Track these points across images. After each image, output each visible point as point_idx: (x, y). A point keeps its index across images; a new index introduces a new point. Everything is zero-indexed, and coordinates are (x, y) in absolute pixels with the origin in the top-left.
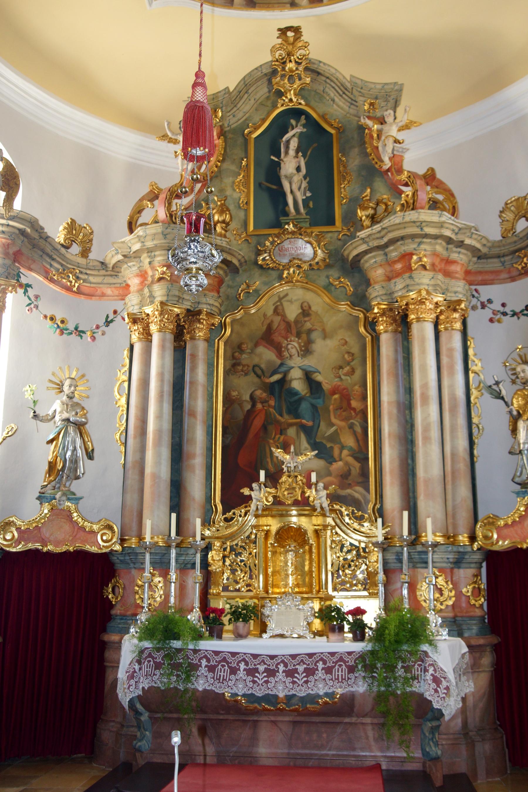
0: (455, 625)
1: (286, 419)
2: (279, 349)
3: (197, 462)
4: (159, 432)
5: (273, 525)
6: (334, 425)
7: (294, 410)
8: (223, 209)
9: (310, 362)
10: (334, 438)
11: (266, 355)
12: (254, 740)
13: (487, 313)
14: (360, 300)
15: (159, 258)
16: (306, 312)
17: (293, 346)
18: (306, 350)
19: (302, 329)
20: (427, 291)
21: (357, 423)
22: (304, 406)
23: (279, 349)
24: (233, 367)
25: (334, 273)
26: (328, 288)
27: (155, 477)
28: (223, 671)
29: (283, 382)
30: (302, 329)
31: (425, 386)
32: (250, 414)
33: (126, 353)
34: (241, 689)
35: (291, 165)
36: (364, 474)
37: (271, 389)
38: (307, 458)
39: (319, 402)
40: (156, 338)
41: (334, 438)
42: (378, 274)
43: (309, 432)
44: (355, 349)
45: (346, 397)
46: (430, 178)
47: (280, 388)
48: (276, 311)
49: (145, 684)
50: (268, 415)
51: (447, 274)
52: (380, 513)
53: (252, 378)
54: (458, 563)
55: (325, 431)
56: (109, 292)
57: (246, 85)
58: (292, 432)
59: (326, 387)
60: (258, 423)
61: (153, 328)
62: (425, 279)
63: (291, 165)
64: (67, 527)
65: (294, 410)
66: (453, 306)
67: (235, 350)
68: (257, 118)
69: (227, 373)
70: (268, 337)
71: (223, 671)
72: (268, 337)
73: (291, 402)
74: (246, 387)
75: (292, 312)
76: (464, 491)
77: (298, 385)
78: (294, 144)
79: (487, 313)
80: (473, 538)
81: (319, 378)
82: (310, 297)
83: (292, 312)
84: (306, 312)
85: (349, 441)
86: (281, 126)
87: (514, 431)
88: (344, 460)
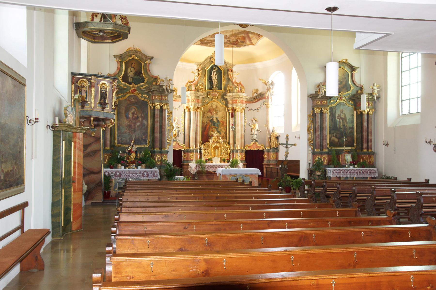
0: (241, 161)
1: (213, 126)
2: (212, 113)
3: (199, 134)
4: (193, 129)
5: (213, 146)
6: (221, 128)
7: (214, 125)
8: (202, 86)
9: (217, 116)
10: (221, 130)
11: (209, 114)
12: (213, 178)
13: (248, 109)
14: (226, 105)
15: (193, 98)
16: (216, 107)
17: (214, 113)
18: (217, 114)
19: (216, 110)
20: (239, 106)
21: (225, 128)
22: (216, 124)
23: (212, 113)
24: (203, 116)
25: (222, 99)
26: (221, 102)
27: (193, 137)
28: (209, 168)
29: (212, 120)
30: (216, 110)
31: (238, 123)
32: (206, 125)
33: (183, 113)
34: (212, 170)
35: (214, 77)
36: (226, 137)
37: (210, 121)
38: (218, 134)
39: (219, 124)
40: (192, 112)
41: (221, 130)
42: (230, 102)
43: (217, 129)
44: (225, 114)
45: (223, 123)
46: (240, 83)
47: (212, 121)
48: (211, 106)
49: (197, 170)
50: (210, 126)
51: (242, 103)
52: (229, 143)
53: (207, 118)
54: (242, 152)
55: (219, 129)
56: (179, 100)
57: (206, 60)
58: (214, 129)
59: (220, 121)
60: (208, 127)
61: (191, 110)
62: (239, 105)
63: (214, 77)
64: (178, 145)
65: (214, 125)
66: (243, 109)
67: (204, 114)
68: (208, 66)
69: (202, 117)
70: (210, 111)
71: (209, 168)
72: (210, 111)
73: (214, 124)
74: (206, 120)
75: (214, 107)
76: (243, 140)
77: (215, 120)
78: (215, 73)
79: (248, 109)
80: (244, 148)
81: (219, 119)
82: (217, 104)
83: (214, 107)
84: (216, 107)
85: (224, 131)
86: (212, 68)
87: (252, 131)
88: (223, 134)
